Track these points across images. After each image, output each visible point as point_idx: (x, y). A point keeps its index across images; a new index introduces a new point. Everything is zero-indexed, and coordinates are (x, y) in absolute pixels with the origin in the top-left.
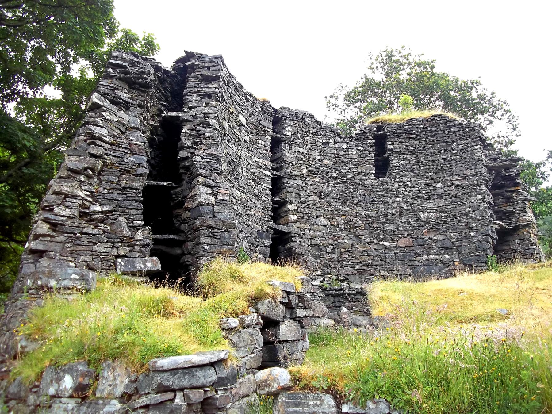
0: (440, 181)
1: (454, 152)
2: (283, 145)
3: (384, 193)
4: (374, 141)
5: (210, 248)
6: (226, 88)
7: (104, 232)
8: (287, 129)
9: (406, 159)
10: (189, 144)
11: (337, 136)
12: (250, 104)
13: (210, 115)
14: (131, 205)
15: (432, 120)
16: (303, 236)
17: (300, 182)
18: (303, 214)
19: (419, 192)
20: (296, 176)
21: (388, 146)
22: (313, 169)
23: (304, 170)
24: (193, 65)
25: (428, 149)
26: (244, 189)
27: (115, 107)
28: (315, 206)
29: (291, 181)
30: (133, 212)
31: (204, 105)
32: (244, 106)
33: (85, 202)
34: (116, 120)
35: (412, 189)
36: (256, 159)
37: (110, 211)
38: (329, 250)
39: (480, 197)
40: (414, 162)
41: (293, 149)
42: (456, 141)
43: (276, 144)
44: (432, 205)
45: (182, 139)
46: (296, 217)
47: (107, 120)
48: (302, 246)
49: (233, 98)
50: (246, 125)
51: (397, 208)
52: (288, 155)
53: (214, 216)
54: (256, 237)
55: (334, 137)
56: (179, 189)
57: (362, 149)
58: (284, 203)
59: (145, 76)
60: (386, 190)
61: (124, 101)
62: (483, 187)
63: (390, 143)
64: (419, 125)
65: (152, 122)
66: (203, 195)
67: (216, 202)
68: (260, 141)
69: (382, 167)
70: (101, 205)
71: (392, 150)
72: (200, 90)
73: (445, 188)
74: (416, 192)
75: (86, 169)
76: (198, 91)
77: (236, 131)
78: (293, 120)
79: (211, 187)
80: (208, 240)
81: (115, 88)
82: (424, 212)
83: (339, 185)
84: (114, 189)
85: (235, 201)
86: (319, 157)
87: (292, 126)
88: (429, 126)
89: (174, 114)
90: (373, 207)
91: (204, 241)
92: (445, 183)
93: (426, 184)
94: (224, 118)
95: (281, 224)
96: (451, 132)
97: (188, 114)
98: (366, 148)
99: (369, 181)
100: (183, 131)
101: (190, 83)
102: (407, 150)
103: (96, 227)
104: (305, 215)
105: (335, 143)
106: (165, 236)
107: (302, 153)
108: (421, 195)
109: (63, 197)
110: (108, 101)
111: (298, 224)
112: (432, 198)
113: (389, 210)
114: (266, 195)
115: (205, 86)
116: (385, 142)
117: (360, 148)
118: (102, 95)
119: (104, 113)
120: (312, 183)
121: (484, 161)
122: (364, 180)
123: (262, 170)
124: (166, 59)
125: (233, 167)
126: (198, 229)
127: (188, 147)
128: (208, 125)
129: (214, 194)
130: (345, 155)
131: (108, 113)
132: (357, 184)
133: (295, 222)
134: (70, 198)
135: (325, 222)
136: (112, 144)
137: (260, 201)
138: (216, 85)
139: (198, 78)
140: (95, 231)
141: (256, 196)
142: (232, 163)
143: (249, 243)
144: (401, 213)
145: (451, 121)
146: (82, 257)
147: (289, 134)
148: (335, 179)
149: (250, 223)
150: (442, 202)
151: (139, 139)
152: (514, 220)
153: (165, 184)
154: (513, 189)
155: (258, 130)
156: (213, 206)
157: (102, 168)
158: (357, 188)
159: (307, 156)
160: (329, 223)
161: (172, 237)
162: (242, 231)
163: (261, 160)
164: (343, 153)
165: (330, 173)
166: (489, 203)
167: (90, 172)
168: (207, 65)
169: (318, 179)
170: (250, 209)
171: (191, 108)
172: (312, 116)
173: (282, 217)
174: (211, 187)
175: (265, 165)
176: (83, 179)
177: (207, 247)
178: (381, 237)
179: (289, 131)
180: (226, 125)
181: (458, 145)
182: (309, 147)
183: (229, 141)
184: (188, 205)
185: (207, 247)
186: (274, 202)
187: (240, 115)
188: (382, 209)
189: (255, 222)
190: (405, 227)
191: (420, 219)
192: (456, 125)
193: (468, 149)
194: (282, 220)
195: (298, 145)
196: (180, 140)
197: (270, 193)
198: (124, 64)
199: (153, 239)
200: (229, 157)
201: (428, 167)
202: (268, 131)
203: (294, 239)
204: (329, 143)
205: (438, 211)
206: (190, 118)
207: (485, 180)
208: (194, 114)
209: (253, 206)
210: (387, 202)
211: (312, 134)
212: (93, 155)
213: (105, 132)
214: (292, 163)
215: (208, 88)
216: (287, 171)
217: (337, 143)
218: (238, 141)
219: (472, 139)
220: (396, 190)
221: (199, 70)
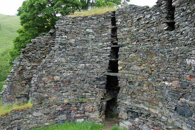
3: (170, 44)
8: (118, 21)
19: (188, 39)
36: (101, 44)
38: (137, 84)
43: (114, 30)
48: (123, 82)
50: (92, 32)
54: (94, 81)
68: (103, 35)
86: (135, 30)
105: (144, 17)
117: (158, 13)
130: (149, 22)
159: (129, 31)
163: (104, 43)
164: (147, 21)
165: (142, 37)
169: (135, 43)
179: (119, 21)
182: (131, 25)
195: (124, 27)
202: (108, 27)
211: (131, 17)
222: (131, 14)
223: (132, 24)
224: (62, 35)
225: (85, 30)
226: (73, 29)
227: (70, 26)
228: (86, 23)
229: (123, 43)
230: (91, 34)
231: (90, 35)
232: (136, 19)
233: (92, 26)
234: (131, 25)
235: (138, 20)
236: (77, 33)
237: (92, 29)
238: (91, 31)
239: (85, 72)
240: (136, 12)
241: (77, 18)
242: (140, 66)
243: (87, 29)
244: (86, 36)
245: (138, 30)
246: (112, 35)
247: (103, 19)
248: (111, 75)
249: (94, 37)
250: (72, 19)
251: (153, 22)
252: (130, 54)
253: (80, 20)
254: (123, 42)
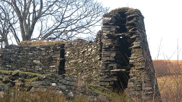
8: (67, 53)
50: (39, 63)
68: (51, 66)
86: (81, 61)
159: (76, 63)
179: (68, 54)
222: (78, 47)
223: (78, 56)
224: (6, 64)
225: (32, 61)
226: (19, 58)
227: (16, 55)
228: (34, 53)
230: (38, 66)
231: (37, 67)
232: (82, 52)
233: (40, 57)
234: (77, 58)
235: (83, 53)
236: (23, 63)
237: (39, 60)
238: (38, 62)
240: (82, 45)
241: (24, 48)
243: (34, 60)
244: (33, 67)
245: (83, 62)
246: (61, 67)
247: (53, 50)
249: (41, 68)
250: (18, 48)
251: (92, 54)
253: (27, 51)
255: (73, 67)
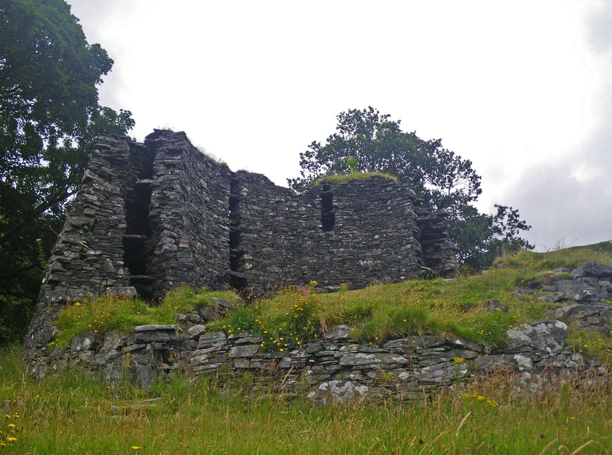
0: (377, 234)
1: (389, 208)
2: (240, 203)
3: (329, 245)
4: (321, 199)
5: (173, 283)
6: (188, 158)
7: (97, 269)
8: (243, 190)
9: (348, 214)
10: (157, 205)
11: (288, 196)
12: (210, 170)
13: (175, 182)
14: (114, 251)
15: (371, 181)
16: (258, 282)
17: (255, 236)
18: (258, 263)
19: (359, 243)
20: (252, 230)
21: (334, 204)
22: (267, 224)
23: (259, 225)
24: (161, 141)
25: (368, 206)
26: (205, 241)
27: (102, 179)
28: (269, 256)
29: (247, 235)
30: (117, 255)
31: (170, 173)
32: (204, 171)
33: (84, 248)
34: (103, 189)
35: (354, 241)
36: (216, 216)
37: (101, 255)
39: (409, 246)
40: (356, 217)
41: (249, 207)
42: (390, 199)
43: (234, 203)
44: (370, 254)
45: (152, 201)
46: (251, 265)
47: (97, 189)
49: (195, 166)
50: (206, 188)
51: (340, 257)
52: (244, 212)
53: (178, 260)
55: (286, 196)
56: (150, 240)
57: (311, 206)
58: (242, 253)
59: (123, 155)
60: (331, 242)
61: (108, 174)
62: (412, 238)
63: (335, 200)
64: (360, 185)
65: (128, 189)
66: (168, 244)
67: (178, 249)
68: (219, 201)
69: (329, 223)
70: (94, 250)
71: (336, 207)
72: (166, 161)
73: (381, 239)
74: (357, 243)
75: (83, 225)
76: (165, 162)
77: (197, 193)
78: (249, 182)
79: (174, 238)
80: (172, 278)
81: (101, 165)
82: (363, 260)
83: (290, 237)
84: (103, 239)
85: (197, 251)
86: (272, 214)
87: (248, 188)
88: (368, 186)
89: (146, 181)
90: (320, 256)
91: (169, 279)
92: (381, 234)
93: (365, 236)
94: (186, 183)
95: (238, 271)
96: (386, 191)
97: (157, 180)
98: (314, 205)
99: (317, 234)
100: (153, 195)
101: (158, 156)
102: (350, 206)
103: (91, 266)
104: (260, 264)
105: (286, 202)
106: (139, 276)
107: (257, 210)
108: (361, 245)
109: (69, 244)
110: (97, 175)
111: (254, 271)
112: (370, 248)
113: (334, 259)
114: (225, 246)
115: (171, 157)
116: (331, 202)
117: (309, 205)
118: (92, 171)
119: (94, 185)
120: (265, 236)
121: (413, 216)
122: (312, 233)
123: (221, 226)
124: (139, 134)
125: (195, 223)
126: (164, 270)
127: (157, 208)
128: (172, 189)
129: (177, 243)
130: (295, 211)
131: (97, 185)
132: (306, 236)
133: (251, 269)
134: (74, 245)
135: (277, 270)
136: (100, 207)
137: (219, 252)
138: (179, 157)
139: (165, 151)
140: (91, 268)
141: (215, 247)
142: (194, 219)
143: (209, 286)
144: (344, 261)
145: (387, 182)
146: (83, 286)
147: (245, 194)
148: (287, 232)
149: (210, 269)
150: (379, 251)
151: (119, 204)
152: (441, 267)
153: (139, 237)
154: (441, 240)
155: (217, 192)
156: (176, 252)
157: (94, 223)
158: (306, 240)
159: (262, 213)
160: (281, 271)
161: (145, 277)
162: (204, 276)
163: (220, 217)
166: (417, 251)
167: (86, 227)
168: (172, 141)
170: (211, 258)
171: (159, 176)
172: (265, 179)
173: (240, 266)
174: (174, 238)
175: (224, 221)
176: (81, 233)
177: (171, 283)
178: (326, 281)
179: (245, 191)
180: (189, 189)
181: (391, 202)
182: (264, 205)
183: (191, 202)
184: (157, 252)
185: (171, 283)
186: (231, 252)
187: (201, 179)
188: (327, 258)
189: (215, 269)
190: (346, 273)
191: (359, 266)
192: (390, 185)
193: (401, 206)
194: (240, 268)
195: (254, 203)
196: (150, 202)
197: (228, 245)
198: (108, 146)
199: (131, 279)
200: (191, 214)
201: (367, 221)
203: (249, 284)
204: (281, 202)
205: (375, 259)
206: (158, 184)
207: (413, 232)
208: (162, 180)
209: (213, 256)
210: (332, 252)
212: (87, 215)
213: (95, 198)
214: (248, 219)
215: (173, 159)
216: (243, 226)
217: (288, 201)
218: (200, 202)
219: (404, 197)
220: (340, 241)
221: (165, 145)
229: (251, 227)
235: (276, 202)
239: (202, 260)
242: (282, 267)
245: (275, 216)
248: (238, 276)
252: (263, 247)
254: (249, 225)
255: (256, 218)
